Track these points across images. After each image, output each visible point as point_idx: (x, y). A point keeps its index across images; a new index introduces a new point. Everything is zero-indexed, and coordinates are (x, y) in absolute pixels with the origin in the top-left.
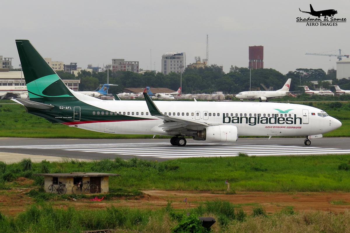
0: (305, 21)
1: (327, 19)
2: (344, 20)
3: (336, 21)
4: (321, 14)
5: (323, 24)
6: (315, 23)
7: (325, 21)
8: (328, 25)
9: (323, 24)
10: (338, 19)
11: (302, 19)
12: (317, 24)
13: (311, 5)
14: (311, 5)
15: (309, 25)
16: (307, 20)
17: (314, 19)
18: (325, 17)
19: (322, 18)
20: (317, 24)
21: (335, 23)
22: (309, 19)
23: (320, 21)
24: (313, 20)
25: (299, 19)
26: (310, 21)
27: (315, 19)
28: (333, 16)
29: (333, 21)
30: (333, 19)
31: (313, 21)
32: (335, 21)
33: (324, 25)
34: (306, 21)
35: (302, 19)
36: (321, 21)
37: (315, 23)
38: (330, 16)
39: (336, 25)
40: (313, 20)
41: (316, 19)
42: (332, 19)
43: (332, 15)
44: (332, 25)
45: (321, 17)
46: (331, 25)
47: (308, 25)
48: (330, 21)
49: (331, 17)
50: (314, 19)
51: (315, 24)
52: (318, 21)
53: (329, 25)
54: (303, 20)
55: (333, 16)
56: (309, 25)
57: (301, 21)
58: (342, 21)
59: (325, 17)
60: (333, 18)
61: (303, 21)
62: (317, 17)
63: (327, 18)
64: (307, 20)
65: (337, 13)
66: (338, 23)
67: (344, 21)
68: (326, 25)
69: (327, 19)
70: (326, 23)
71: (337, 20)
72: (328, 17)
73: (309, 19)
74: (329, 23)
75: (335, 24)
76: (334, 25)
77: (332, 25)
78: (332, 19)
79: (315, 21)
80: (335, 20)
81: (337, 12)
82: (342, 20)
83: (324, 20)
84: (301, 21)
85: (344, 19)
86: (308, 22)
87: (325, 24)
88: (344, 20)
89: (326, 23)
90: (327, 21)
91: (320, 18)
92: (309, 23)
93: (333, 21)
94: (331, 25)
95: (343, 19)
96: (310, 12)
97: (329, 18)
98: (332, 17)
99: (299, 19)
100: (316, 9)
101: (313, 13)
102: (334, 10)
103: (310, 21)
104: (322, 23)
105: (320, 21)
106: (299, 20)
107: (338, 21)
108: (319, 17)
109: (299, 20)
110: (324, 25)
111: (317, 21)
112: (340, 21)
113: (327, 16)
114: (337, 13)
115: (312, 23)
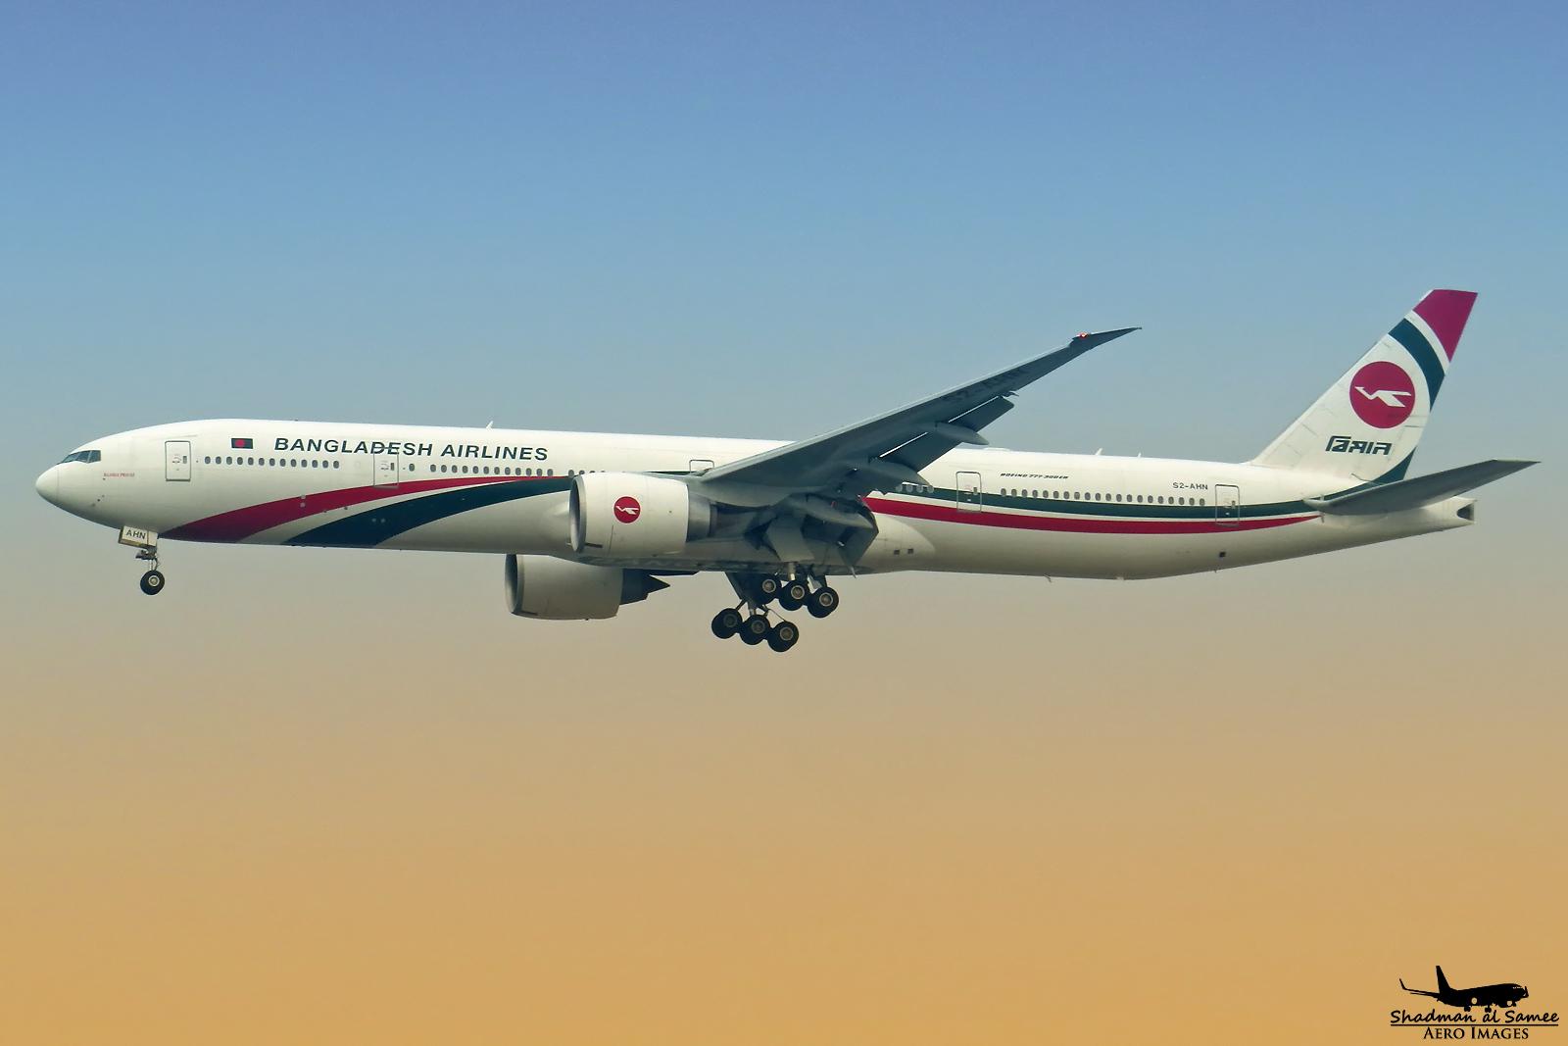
0: (1420, 1022)
1: (1494, 1018)
2: (1552, 1019)
3: (1525, 1022)
5: (1480, 1032)
6: (1453, 1029)
7: (1487, 1023)
8: (1495, 1037)
9: (1480, 1032)
10: (1532, 1016)
11: (1409, 1016)
12: (1459, 1033)
13: (1438, 968)
14: (1438, 968)
15: (1434, 1035)
16: (1426, 1019)
17: (1449, 1016)
18: (1488, 1010)
19: (1477, 1012)
20: (1459, 1033)
21: (1522, 1028)
22: (1432, 1015)
23: (1469, 1022)
24: (1445, 1020)
25: (1400, 1016)
26: (1437, 1022)
28: (1514, 1005)
29: (1514, 1022)
30: (1515, 1016)
31: (1448, 1022)
32: (1521, 1022)
33: (1483, 1037)
34: (1424, 1022)
35: (1409, 1016)
36: (1475, 1023)
37: (1453, 1029)
38: (1504, 1005)
39: (1525, 1036)
40: (1445, 1020)
41: (1458, 1017)
42: (1509, 1014)
43: (1510, 1003)
44: (1510, 1035)
46: (1506, 1035)
47: (1428, 1036)
48: (1502, 1022)
49: (1507, 1009)
50: (1449, 1016)
51: (1452, 1034)
52: (1463, 1022)
53: (1500, 1035)
55: (1514, 1005)
56: (1434, 1035)
57: (1407, 1022)
58: (1543, 1022)
60: (1513, 1012)
61: (1413, 1023)
62: (1461, 1010)
63: (1493, 1011)
64: (1426, 1019)
65: (1527, 996)
66: (1531, 1030)
67: (1551, 1022)
68: (1490, 1034)
69: (1494, 1018)
70: (1491, 1030)
71: (1528, 1019)
72: (1498, 1008)
74: (1499, 1029)
75: (1521, 1031)
76: (1518, 1036)
77: (1510, 1035)
79: (1453, 1022)
80: (1521, 1018)
81: (1526, 991)
82: (1544, 1019)
83: (1484, 1021)
84: (1407, 1022)
88: (1552, 1019)
89: (1491, 1030)
90: (1492, 1022)
91: (1469, 1014)
92: (1433, 1029)
93: (1514, 1022)
94: (1507, 1036)
95: (1547, 1014)
96: (1438, 991)
97: (1500, 1012)
98: (1512, 1008)
99: (1400, 1016)
100: (1456, 984)
101: (1447, 994)
102: (1515, 985)
103: (1437, 1022)
104: (1477, 1029)
105: (1469, 1022)
106: (1399, 1019)
107: (1531, 1022)
108: (1467, 1009)
109: (1399, 1019)
110: (1483, 1037)
111: (1459, 1022)
112: (1537, 1022)
113: (1493, 1007)
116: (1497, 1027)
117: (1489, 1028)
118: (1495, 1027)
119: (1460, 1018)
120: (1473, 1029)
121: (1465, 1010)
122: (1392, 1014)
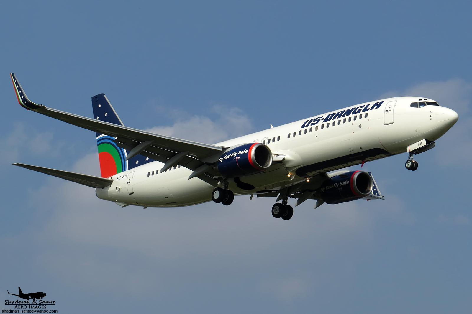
0: (14, 304)
1: (36, 302)
2: (53, 303)
3: (45, 304)
4: (30, 297)
5: (32, 306)
6: (23, 306)
8: (36, 308)
9: (32, 306)
10: (47, 302)
11: (10, 302)
13: (19, 287)
14: (19, 287)
15: (18, 307)
16: (15, 303)
17: (22, 302)
18: (34, 300)
19: (31, 301)
21: (44, 305)
22: (17, 301)
23: (28, 304)
24: (21, 303)
26: (19, 304)
27: (23, 302)
28: (42, 298)
29: (42, 304)
30: (42, 302)
31: (22, 304)
32: (44, 304)
33: (33, 308)
34: (15, 304)
35: (10, 302)
37: (23, 306)
38: (39, 299)
39: (45, 308)
40: (21, 303)
41: (25, 302)
42: (40, 301)
43: (41, 298)
45: (29, 299)
46: (39, 307)
47: (16, 308)
48: (38, 304)
49: (40, 300)
50: (22, 302)
51: (23, 307)
52: (26, 304)
54: (12, 303)
55: (42, 298)
56: (18, 307)
57: (10, 303)
58: (50, 304)
59: (34, 300)
60: (42, 301)
61: (12, 304)
62: (26, 300)
65: (46, 296)
66: (47, 306)
67: (53, 304)
68: (35, 308)
69: (36, 302)
70: (35, 306)
71: (46, 302)
73: (17, 302)
74: (37, 306)
76: (43, 308)
78: (40, 301)
79: (23, 304)
80: (44, 302)
83: (33, 303)
84: (10, 303)
85: (53, 302)
86: (17, 305)
87: (34, 307)
88: (53, 303)
89: (35, 306)
90: (35, 304)
91: (28, 301)
92: (18, 306)
93: (42, 304)
96: (19, 294)
97: (38, 301)
98: (41, 299)
99: (8, 302)
100: (25, 292)
101: (22, 295)
103: (19, 304)
104: (31, 306)
105: (28, 304)
106: (7, 303)
107: (47, 304)
108: (28, 300)
110: (33, 308)
111: (25, 304)
112: (49, 304)
113: (36, 299)
114: (46, 296)
115: (21, 306)
116: (37, 305)
117: (34, 305)
118: (36, 305)
119: (26, 302)
120: (30, 306)
121: (27, 300)
122: (5, 301)
